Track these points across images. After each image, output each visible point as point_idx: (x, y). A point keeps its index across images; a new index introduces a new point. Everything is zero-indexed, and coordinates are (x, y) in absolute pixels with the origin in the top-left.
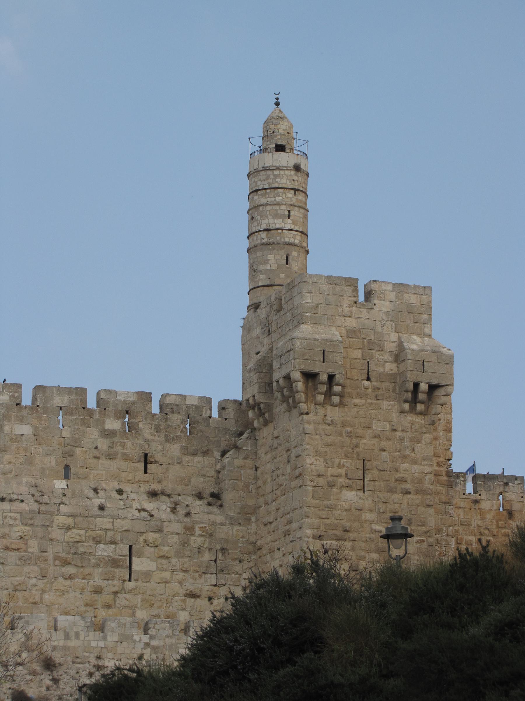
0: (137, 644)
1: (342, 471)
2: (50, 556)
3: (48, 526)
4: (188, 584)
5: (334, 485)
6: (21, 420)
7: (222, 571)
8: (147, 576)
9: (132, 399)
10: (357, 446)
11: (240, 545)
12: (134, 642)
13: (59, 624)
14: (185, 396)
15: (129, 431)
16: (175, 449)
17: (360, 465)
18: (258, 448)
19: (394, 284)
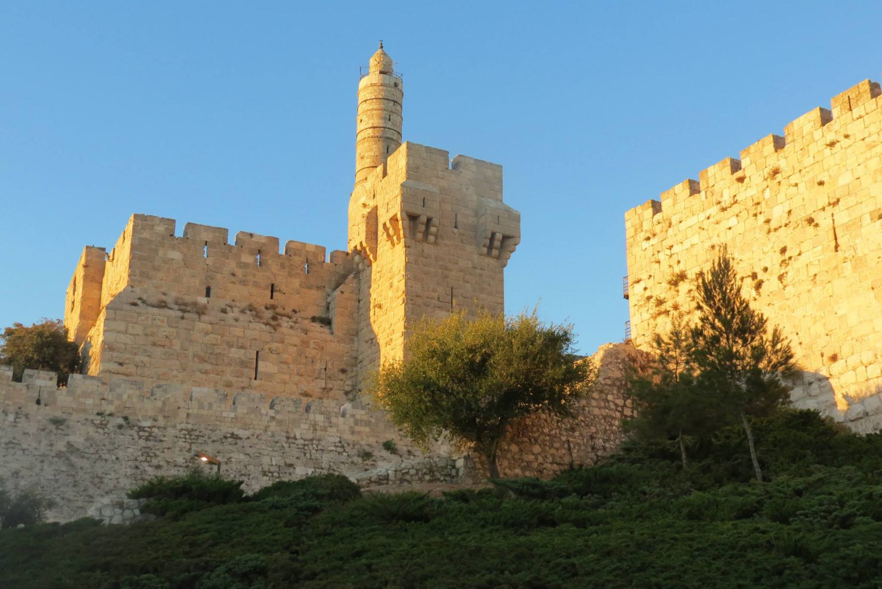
0: (264, 417)
1: (436, 295)
2: (190, 353)
3: (191, 330)
4: (302, 386)
5: (429, 306)
6: (173, 248)
7: (330, 377)
8: (269, 376)
9: (263, 241)
10: (446, 277)
11: (345, 359)
12: (262, 415)
13: (194, 395)
14: (305, 244)
15: (260, 265)
16: (296, 282)
17: (449, 292)
18: (362, 284)
19: (476, 160)
